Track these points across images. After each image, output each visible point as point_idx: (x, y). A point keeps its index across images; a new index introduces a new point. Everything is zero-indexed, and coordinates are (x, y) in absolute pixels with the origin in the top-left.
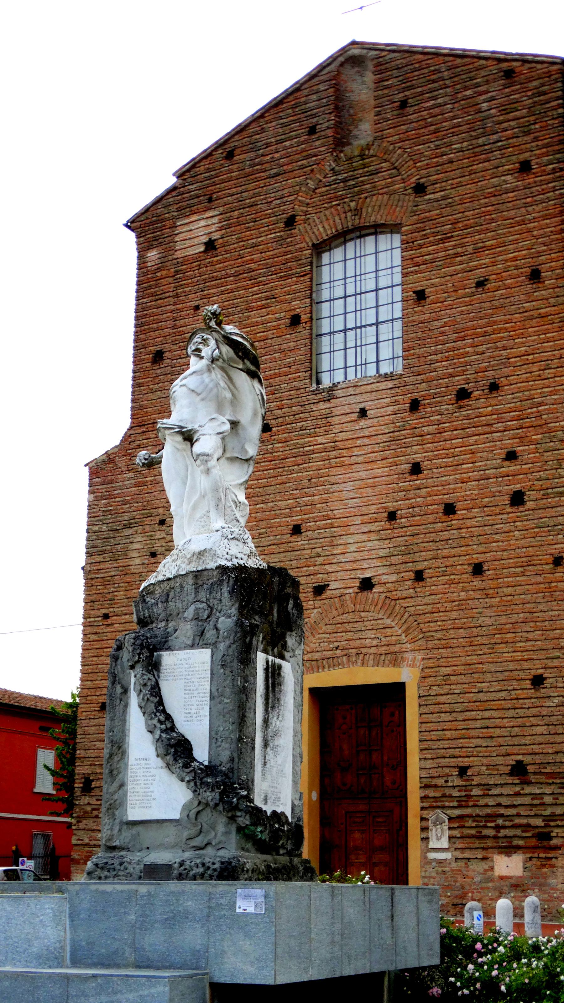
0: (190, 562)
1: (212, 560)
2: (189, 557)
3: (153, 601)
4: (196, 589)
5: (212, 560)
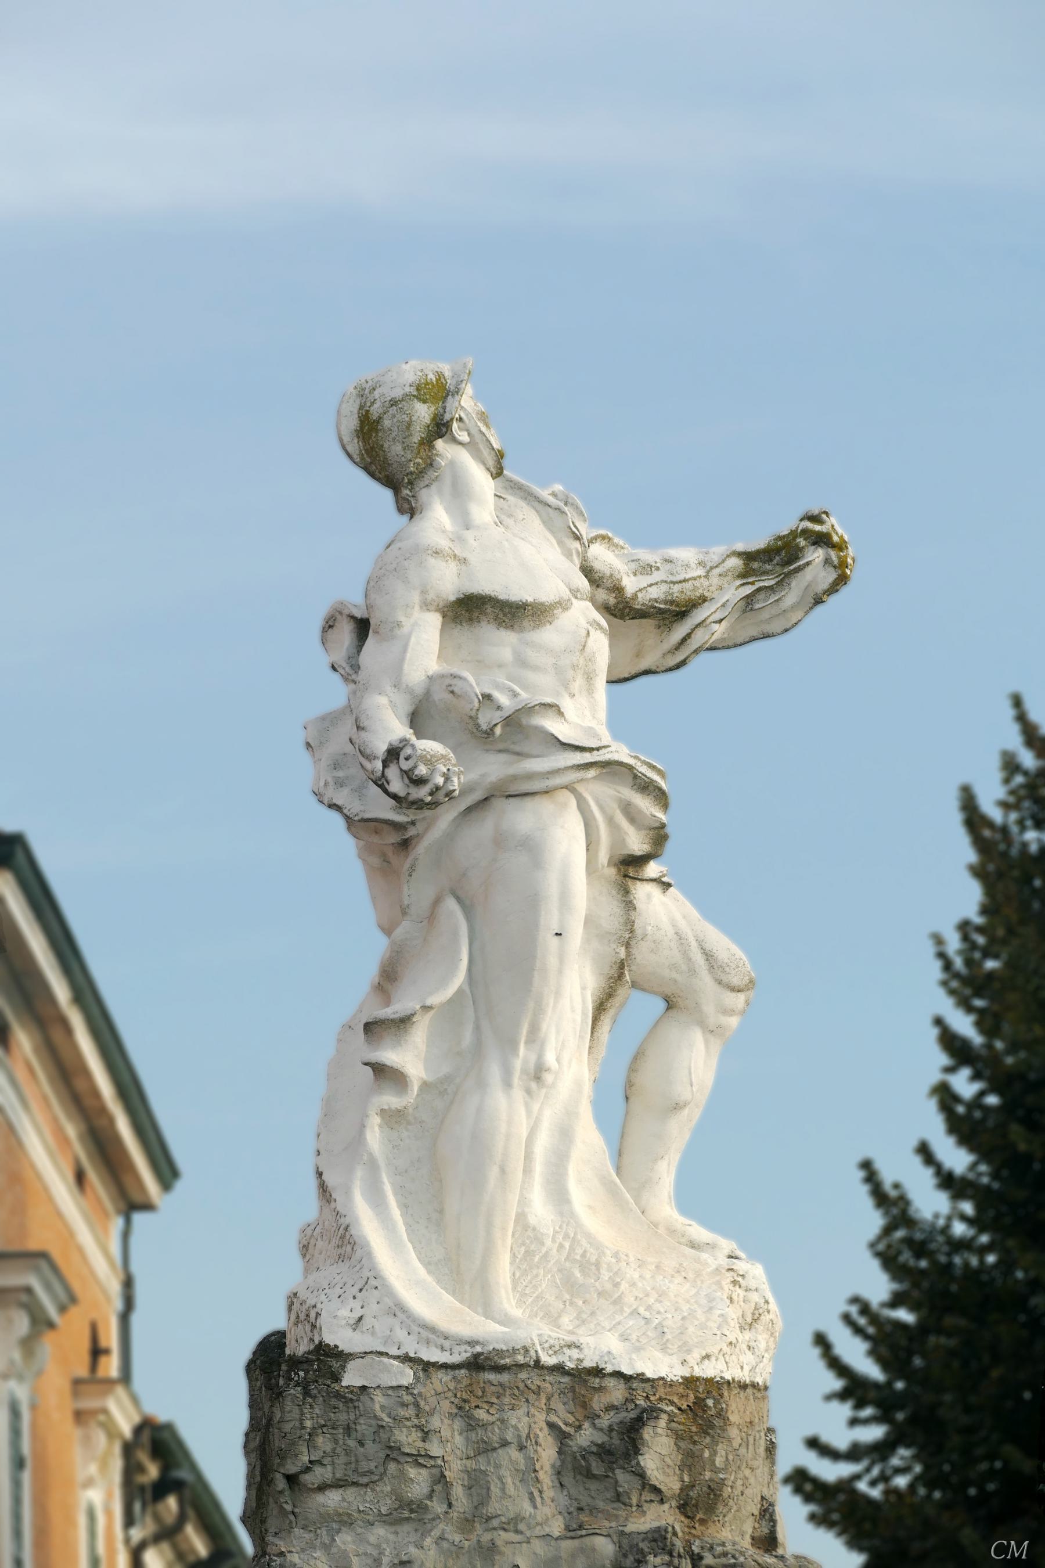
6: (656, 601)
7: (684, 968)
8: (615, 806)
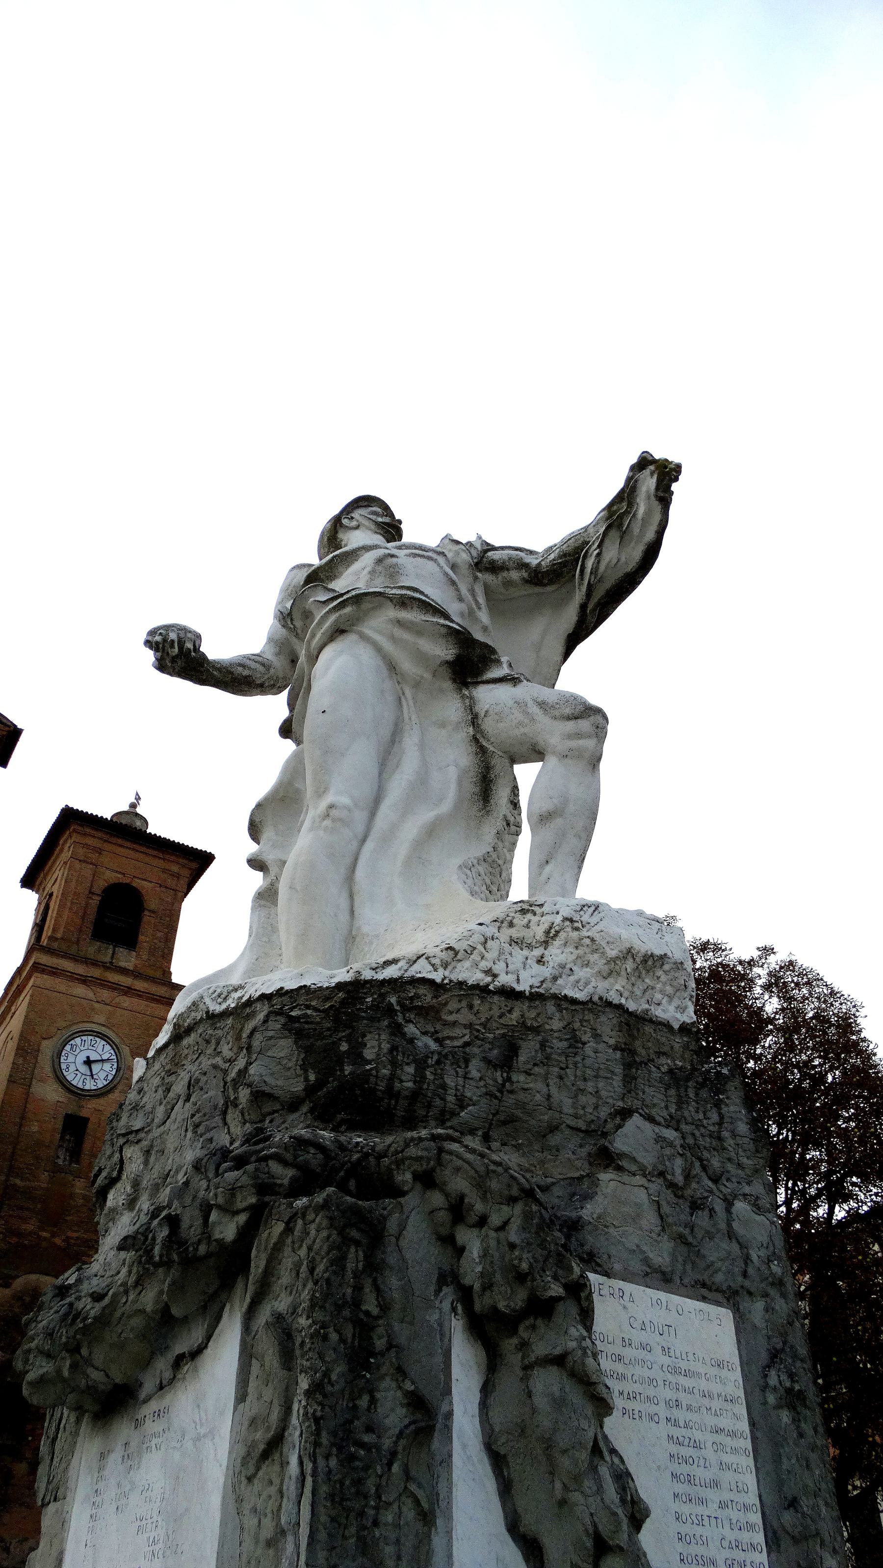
0: (610, 973)
1: (671, 998)
2: (612, 953)
3: (433, 1046)
4: (628, 1066)
5: (671, 998)
6: (554, 560)
7: (526, 721)
8: (390, 626)
